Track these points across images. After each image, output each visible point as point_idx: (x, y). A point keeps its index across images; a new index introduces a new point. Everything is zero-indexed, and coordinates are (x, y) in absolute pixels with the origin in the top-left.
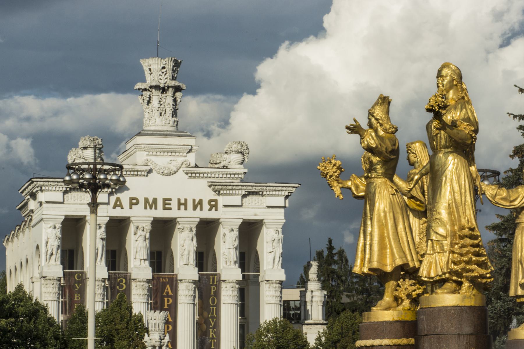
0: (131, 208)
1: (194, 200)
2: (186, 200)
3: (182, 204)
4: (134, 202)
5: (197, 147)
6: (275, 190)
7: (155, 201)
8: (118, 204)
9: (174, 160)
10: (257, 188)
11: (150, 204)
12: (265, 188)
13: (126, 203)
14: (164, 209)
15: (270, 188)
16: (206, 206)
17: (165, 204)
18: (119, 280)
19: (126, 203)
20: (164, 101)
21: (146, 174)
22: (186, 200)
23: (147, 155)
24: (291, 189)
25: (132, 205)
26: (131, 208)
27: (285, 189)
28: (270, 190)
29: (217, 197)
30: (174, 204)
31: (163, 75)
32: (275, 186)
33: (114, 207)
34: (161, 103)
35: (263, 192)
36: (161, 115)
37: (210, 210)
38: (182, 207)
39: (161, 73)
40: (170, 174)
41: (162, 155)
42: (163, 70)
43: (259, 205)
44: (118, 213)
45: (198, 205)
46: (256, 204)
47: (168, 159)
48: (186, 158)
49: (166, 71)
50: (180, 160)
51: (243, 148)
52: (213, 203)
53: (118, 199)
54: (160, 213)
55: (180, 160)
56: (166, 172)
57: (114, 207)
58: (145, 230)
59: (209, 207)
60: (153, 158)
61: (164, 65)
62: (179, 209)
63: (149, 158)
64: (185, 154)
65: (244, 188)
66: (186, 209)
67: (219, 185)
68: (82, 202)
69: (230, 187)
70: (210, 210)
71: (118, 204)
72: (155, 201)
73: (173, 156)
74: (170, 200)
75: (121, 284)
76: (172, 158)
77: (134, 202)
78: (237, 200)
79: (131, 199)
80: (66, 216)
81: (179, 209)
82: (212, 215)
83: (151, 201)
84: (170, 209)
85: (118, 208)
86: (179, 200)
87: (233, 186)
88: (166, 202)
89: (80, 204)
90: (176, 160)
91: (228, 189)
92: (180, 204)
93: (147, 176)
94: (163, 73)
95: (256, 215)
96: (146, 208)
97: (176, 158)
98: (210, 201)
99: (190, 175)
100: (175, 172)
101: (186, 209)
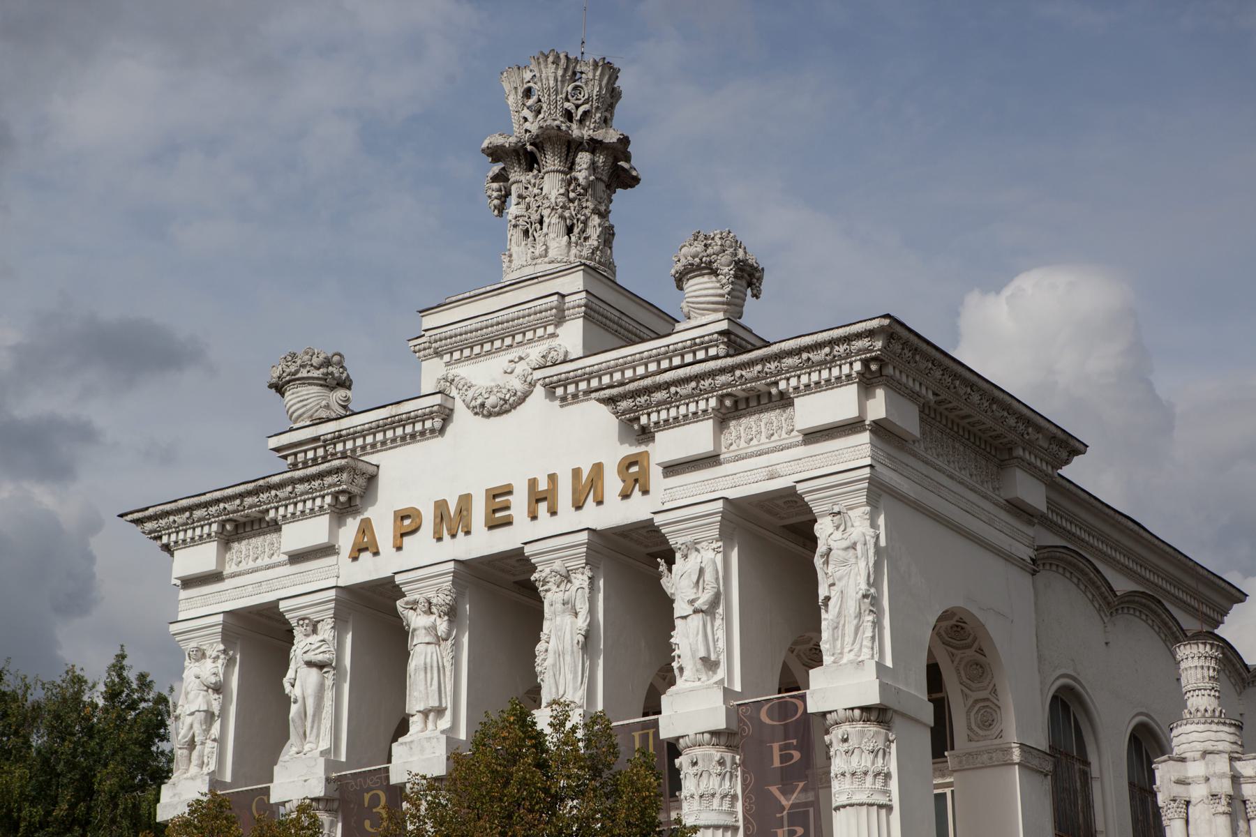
1: (576, 473)
2: (552, 478)
3: (541, 497)
6: (811, 366)
8: (365, 546)
9: (521, 358)
12: (772, 366)
13: (384, 534)
14: (491, 528)
15: (789, 361)
16: (613, 483)
18: (367, 797)
19: (384, 534)
20: (536, 191)
21: (438, 423)
22: (552, 478)
23: (448, 364)
24: (865, 343)
25: (402, 535)
26: (399, 548)
27: (840, 349)
28: (797, 368)
30: (519, 503)
31: (530, 118)
32: (808, 348)
37: (625, 496)
39: (526, 113)
40: (505, 407)
41: (489, 353)
43: (784, 435)
44: (366, 570)
46: (773, 438)
47: (501, 361)
48: (554, 343)
49: (539, 100)
50: (535, 353)
51: (710, 251)
52: (634, 469)
53: (366, 528)
55: (535, 353)
56: (492, 400)
58: (434, 609)
59: (620, 485)
60: (465, 371)
61: (531, 84)
64: (550, 329)
65: (706, 383)
66: (553, 513)
67: (624, 397)
68: (275, 559)
69: (660, 396)
70: (625, 496)
71: (365, 546)
73: (520, 344)
74: (508, 491)
75: (374, 810)
76: (514, 354)
77: (407, 523)
79: (402, 516)
80: (228, 614)
82: (636, 510)
83: (452, 508)
84: (508, 522)
85: (365, 556)
86: (533, 483)
87: (667, 385)
88: (499, 497)
89: (268, 567)
90: (528, 355)
91: (659, 404)
92: (537, 498)
93: (442, 431)
98: (630, 462)
99: (559, 391)
100: (522, 400)
101: (553, 513)
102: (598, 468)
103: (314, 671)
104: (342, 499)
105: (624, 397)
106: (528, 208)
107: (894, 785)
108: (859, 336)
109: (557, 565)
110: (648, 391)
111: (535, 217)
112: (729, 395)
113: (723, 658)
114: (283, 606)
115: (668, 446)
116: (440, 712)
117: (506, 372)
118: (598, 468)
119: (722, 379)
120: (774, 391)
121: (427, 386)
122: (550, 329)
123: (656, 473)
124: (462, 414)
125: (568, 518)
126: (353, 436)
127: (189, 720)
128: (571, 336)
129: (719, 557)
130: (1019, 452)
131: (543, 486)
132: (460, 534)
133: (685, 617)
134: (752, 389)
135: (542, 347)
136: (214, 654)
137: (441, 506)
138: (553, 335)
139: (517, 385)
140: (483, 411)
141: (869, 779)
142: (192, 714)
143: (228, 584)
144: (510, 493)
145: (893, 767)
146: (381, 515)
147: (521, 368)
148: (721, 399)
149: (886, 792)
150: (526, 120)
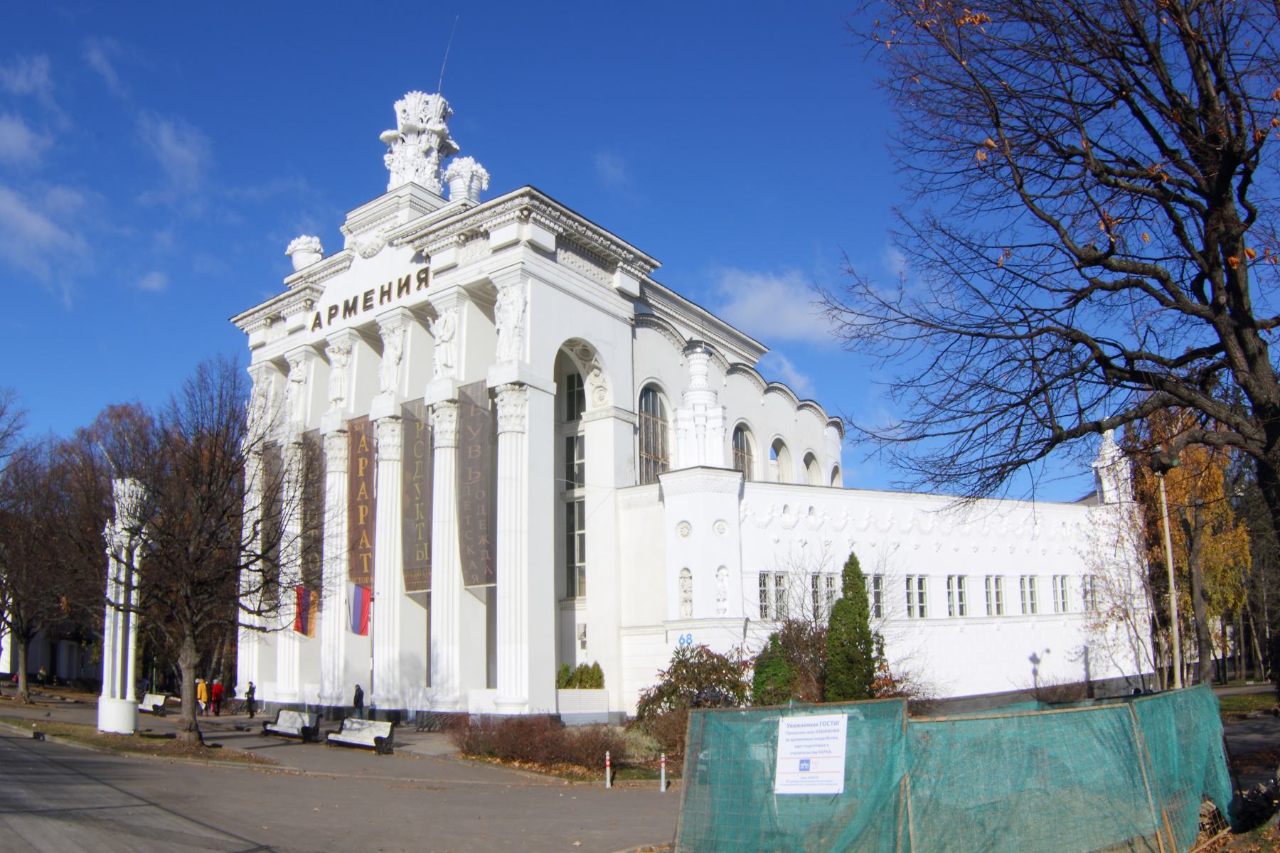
1: (400, 280)
2: (390, 284)
3: (386, 293)
10: (470, 221)
11: (350, 309)
12: (479, 217)
16: (414, 283)
17: (366, 300)
22: (390, 284)
26: (329, 322)
29: (424, 266)
30: (376, 297)
33: (313, 330)
38: (386, 298)
44: (319, 335)
45: (404, 286)
53: (318, 317)
55: (388, 226)
57: (313, 330)
65: (451, 228)
69: (431, 237)
70: (419, 288)
74: (372, 292)
76: (380, 228)
84: (371, 307)
85: (317, 329)
86: (382, 287)
87: (434, 231)
88: (368, 296)
92: (383, 294)
95: (480, 273)
97: (383, 226)
100: (381, 248)
101: (389, 299)
102: (408, 278)
103: (296, 384)
104: (309, 302)
105: (416, 239)
107: (526, 421)
108: (516, 197)
110: (426, 235)
111: (402, 166)
112: (463, 234)
113: (455, 365)
114: (286, 356)
116: (341, 399)
118: (408, 278)
119: (458, 225)
121: (346, 245)
123: (431, 275)
129: (456, 316)
130: (621, 264)
131: (386, 288)
134: (472, 230)
137: (347, 303)
138: (396, 217)
140: (366, 256)
141: (513, 419)
145: (527, 413)
146: (322, 306)
148: (459, 235)
149: (524, 426)
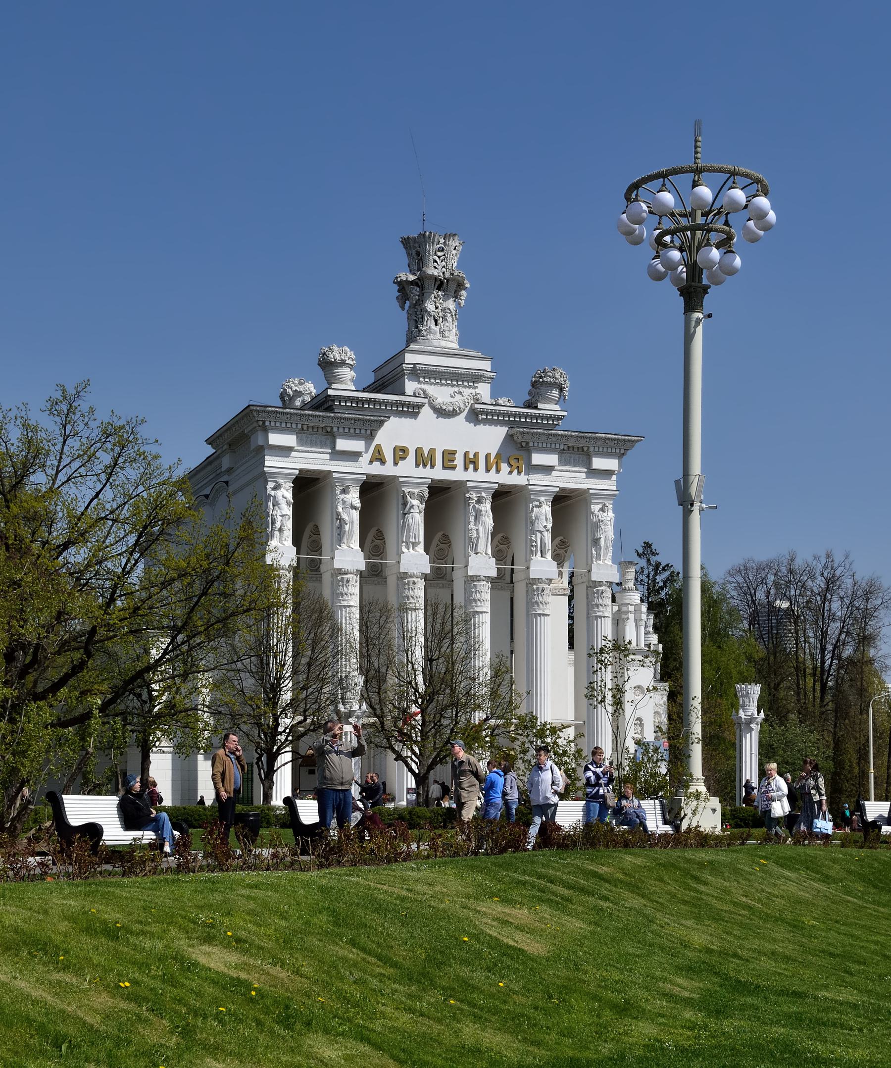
0: (396, 464)
2: (476, 455)
3: (471, 462)
4: (400, 453)
5: (495, 374)
7: (432, 452)
8: (379, 457)
9: (460, 393)
11: (424, 459)
13: (389, 455)
14: (444, 467)
19: (389, 455)
22: (476, 455)
26: (396, 464)
30: (459, 461)
33: (371, 462)
34: (438, 304)
35: (589, 448)
36: (436, 324)
37: (510, 473)
39: (437, 258)
42: (439, 254)
44: (377, 469)
48: (478, 391)
49: (444, 255)
53: (379, 450)
54: (439, 473)
55: (467, 392)
60: (431, 390)
62: (466, 469)
63: (426, 387)
66: (476, 469)
70: (510, 473)
72: (432, 452)
73: (458, 386)
74: (453, 453)
76: (456, 389)
78: (551, 459)
80: (301, 470)
81: (466, 469)
84: (453, 468)
85: (377, 464)
88: (449, 457)
94: (439, 257)
96: (417, 465)
97: (462, 390)
101: (476, 469)
106: (437, 308)
109: (483, 494)
111: (441, 314)
115: (538, 459)
116: (419, 543)
117: (452, 397)
120: (585, 449)
122: (475, 385)
124: (426, 411)
125: (481, 475)
126: (375, 402)
127: (280, 518)
128: (484, 390)
131: (471, 456)
132: (429, 466)
133: (541, 532)
135: (473, 391)
136: (288, 488)
137: (419, 451)
138: (477, 387)
139: (462, 406)
142: (282, 516)
143: (293, 454)
144: (455, 454)
147: (458, 397)
150: (436, 262)
